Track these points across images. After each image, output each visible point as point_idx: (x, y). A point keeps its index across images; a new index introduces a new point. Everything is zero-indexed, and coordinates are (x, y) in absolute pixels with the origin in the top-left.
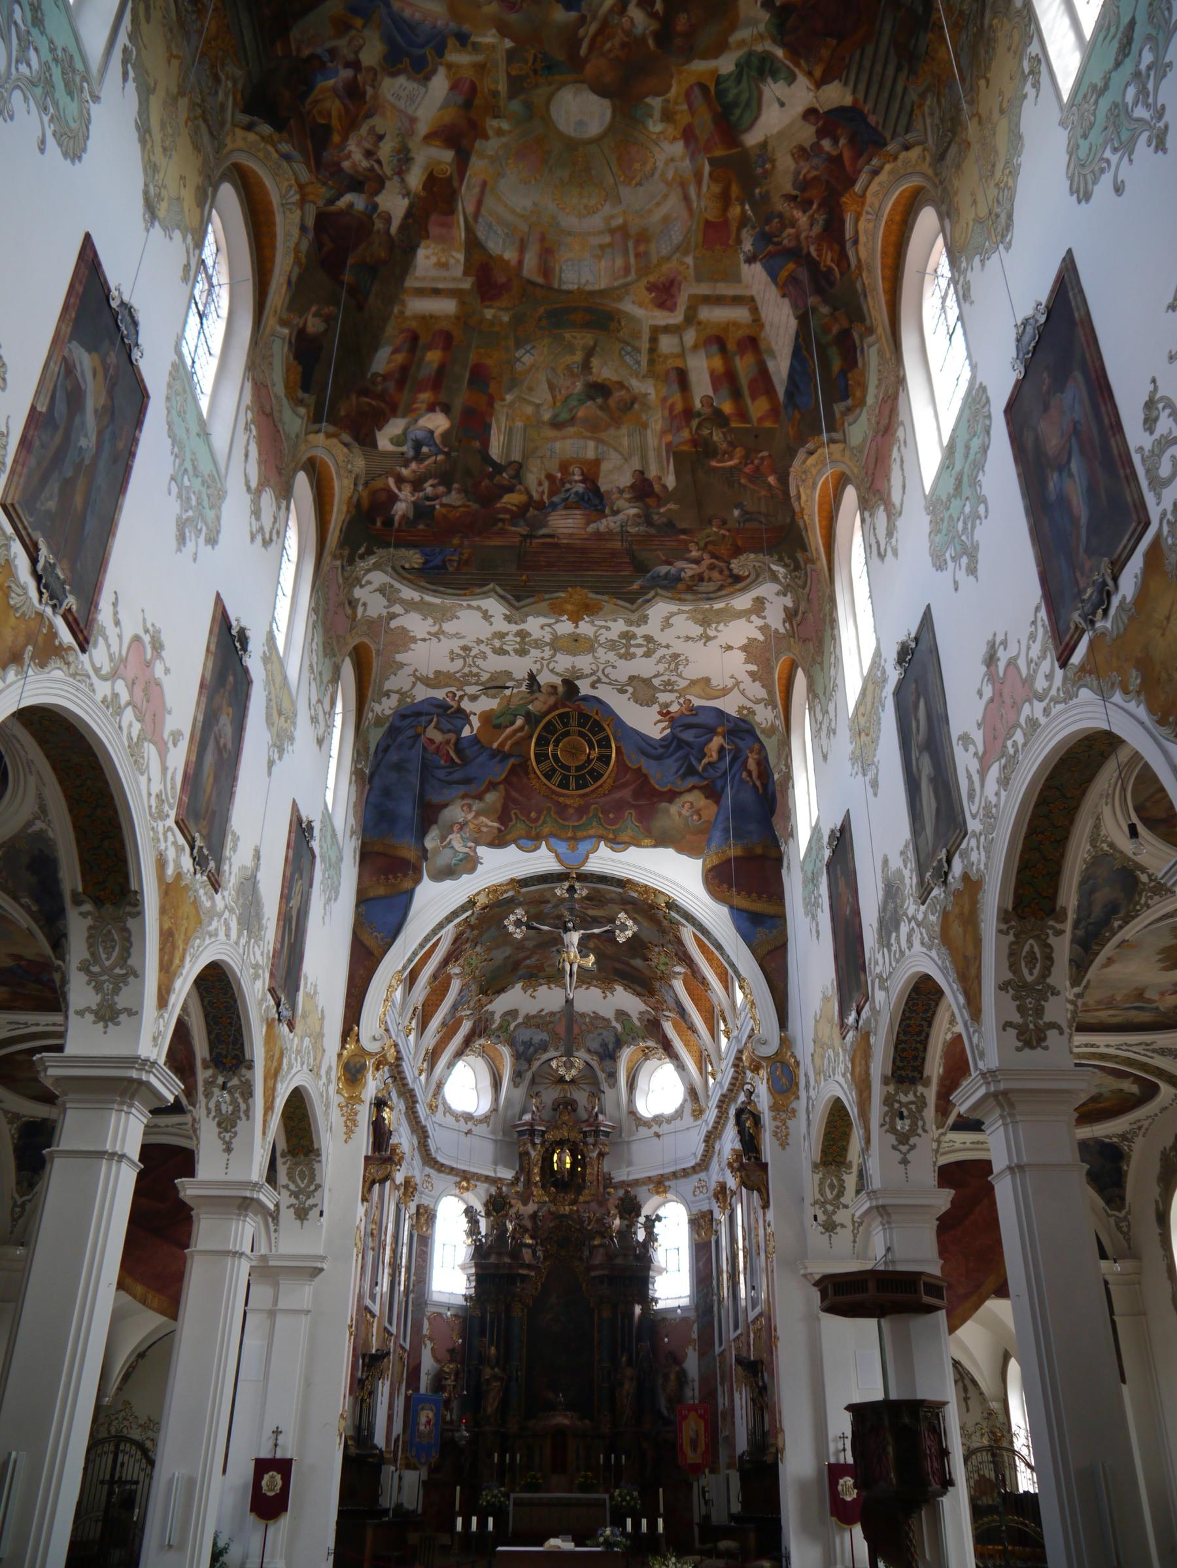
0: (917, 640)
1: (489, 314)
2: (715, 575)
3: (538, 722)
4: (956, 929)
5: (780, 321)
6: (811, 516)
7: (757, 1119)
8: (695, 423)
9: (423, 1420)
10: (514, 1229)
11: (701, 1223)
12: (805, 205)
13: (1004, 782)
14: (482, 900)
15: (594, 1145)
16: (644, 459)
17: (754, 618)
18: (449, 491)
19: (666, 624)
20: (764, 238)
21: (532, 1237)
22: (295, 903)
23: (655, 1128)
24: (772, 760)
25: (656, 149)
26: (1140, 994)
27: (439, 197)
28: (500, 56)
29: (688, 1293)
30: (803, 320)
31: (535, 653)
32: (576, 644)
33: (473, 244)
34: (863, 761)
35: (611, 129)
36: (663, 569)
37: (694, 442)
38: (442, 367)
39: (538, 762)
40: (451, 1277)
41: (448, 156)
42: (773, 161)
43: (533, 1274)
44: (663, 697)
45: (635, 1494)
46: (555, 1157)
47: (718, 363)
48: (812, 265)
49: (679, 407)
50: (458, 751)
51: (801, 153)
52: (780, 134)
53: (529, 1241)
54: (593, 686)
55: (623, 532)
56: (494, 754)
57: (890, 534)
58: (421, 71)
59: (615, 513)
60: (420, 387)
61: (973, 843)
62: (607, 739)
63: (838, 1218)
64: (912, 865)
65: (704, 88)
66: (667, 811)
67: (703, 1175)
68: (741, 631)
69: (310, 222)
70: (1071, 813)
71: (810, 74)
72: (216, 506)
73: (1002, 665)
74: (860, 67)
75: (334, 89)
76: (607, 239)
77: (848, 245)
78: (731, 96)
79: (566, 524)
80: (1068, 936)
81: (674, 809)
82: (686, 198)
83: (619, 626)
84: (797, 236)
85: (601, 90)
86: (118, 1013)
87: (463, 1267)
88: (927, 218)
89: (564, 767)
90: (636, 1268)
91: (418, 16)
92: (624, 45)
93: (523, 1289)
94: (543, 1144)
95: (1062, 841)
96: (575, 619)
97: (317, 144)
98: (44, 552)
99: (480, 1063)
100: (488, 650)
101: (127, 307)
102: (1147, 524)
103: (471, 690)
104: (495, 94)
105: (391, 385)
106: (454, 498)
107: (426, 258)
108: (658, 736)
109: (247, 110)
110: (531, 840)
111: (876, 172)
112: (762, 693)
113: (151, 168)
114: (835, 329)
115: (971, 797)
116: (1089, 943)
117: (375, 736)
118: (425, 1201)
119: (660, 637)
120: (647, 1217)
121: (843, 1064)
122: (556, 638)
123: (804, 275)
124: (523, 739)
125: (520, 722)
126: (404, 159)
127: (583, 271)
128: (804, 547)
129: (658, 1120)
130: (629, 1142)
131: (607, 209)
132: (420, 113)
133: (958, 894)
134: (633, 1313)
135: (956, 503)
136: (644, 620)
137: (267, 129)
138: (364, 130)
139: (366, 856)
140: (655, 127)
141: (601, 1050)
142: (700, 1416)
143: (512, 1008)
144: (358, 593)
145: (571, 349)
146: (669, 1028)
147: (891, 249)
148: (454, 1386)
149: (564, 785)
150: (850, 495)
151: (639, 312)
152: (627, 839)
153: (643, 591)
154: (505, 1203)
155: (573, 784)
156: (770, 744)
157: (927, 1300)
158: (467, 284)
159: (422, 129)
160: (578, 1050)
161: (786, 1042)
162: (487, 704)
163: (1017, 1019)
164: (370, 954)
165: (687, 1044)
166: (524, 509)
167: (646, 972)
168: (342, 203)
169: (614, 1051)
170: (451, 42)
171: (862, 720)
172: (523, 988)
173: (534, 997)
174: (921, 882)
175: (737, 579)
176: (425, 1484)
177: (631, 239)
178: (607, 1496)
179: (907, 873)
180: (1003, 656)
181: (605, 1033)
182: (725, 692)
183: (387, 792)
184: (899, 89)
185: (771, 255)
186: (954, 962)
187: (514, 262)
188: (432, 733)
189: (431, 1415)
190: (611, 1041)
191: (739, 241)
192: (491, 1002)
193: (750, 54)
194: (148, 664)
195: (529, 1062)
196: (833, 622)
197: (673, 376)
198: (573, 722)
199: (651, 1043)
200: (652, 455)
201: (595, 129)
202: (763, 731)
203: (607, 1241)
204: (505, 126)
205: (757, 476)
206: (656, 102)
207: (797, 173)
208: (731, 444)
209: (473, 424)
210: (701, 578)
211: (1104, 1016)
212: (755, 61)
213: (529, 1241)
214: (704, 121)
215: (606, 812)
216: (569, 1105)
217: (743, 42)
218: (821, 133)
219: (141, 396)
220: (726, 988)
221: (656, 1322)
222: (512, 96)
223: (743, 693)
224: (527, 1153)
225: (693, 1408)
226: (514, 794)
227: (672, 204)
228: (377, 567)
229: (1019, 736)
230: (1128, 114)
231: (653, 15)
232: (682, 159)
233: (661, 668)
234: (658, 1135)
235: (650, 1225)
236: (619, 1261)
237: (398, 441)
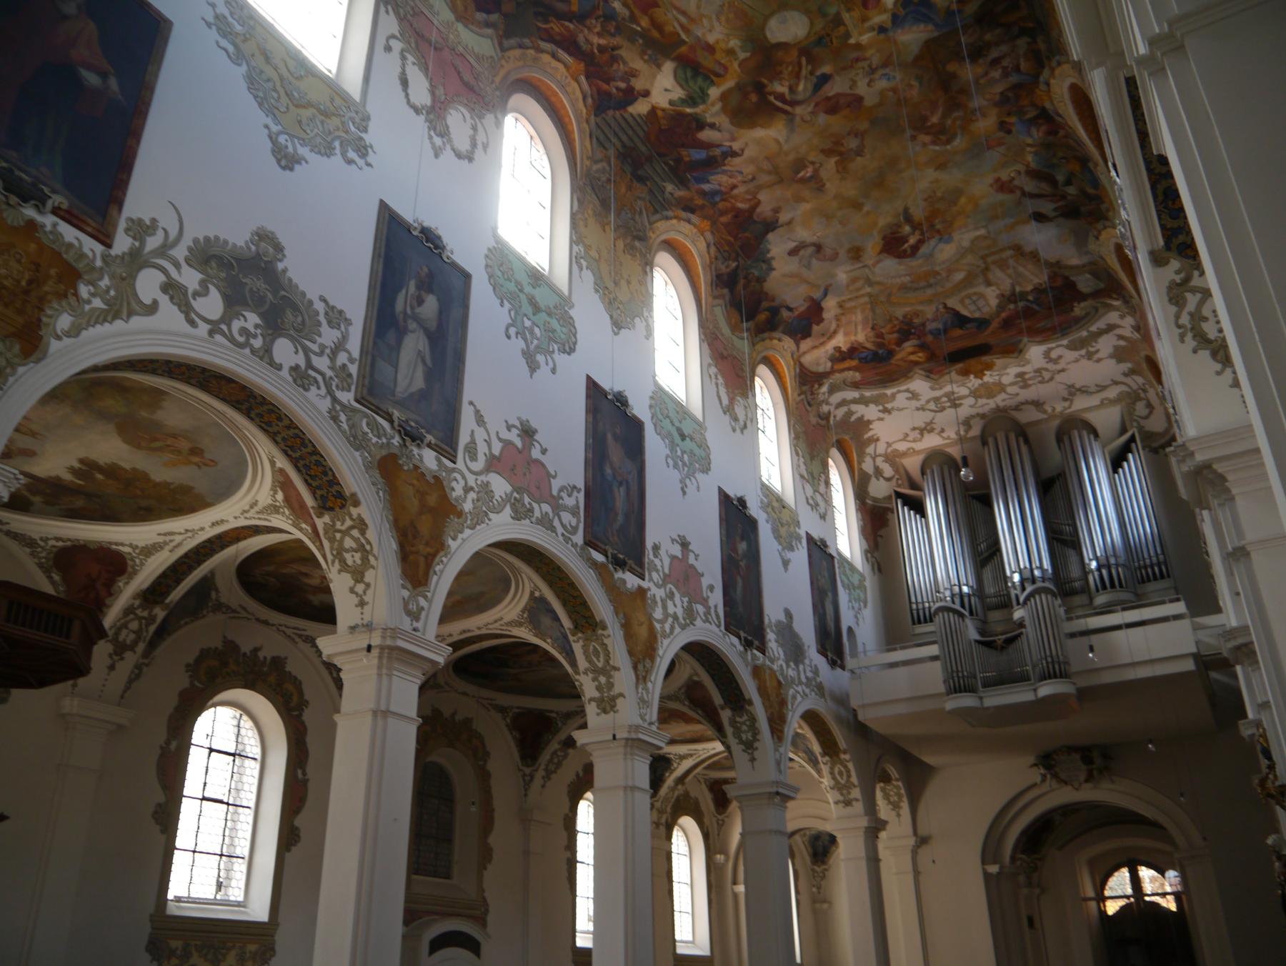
12: (602, 49)
28: (854, 33)
35: (762, 28)
42: (645, 61)
48: (561, 16)
51: (633, 74)
52: (654, 77)
65: (718, 75)
71: (663, 110)
77: (554, 47)
78: (700, 80)
82: (684, 13)
84: (589, 29)
91: (915, 28)
92: (781, 72)
104: (849, 10)
111: (584, 98)
140: (734, 43)
170: (889, 24)
191: (625, 5)
193: (704, 102)
201: (773, 23)
207: (625, 63)
214: (706, 61)
217: (713, 104)
222: (838, 14)
231: (770, 94)
232: (704, 34)
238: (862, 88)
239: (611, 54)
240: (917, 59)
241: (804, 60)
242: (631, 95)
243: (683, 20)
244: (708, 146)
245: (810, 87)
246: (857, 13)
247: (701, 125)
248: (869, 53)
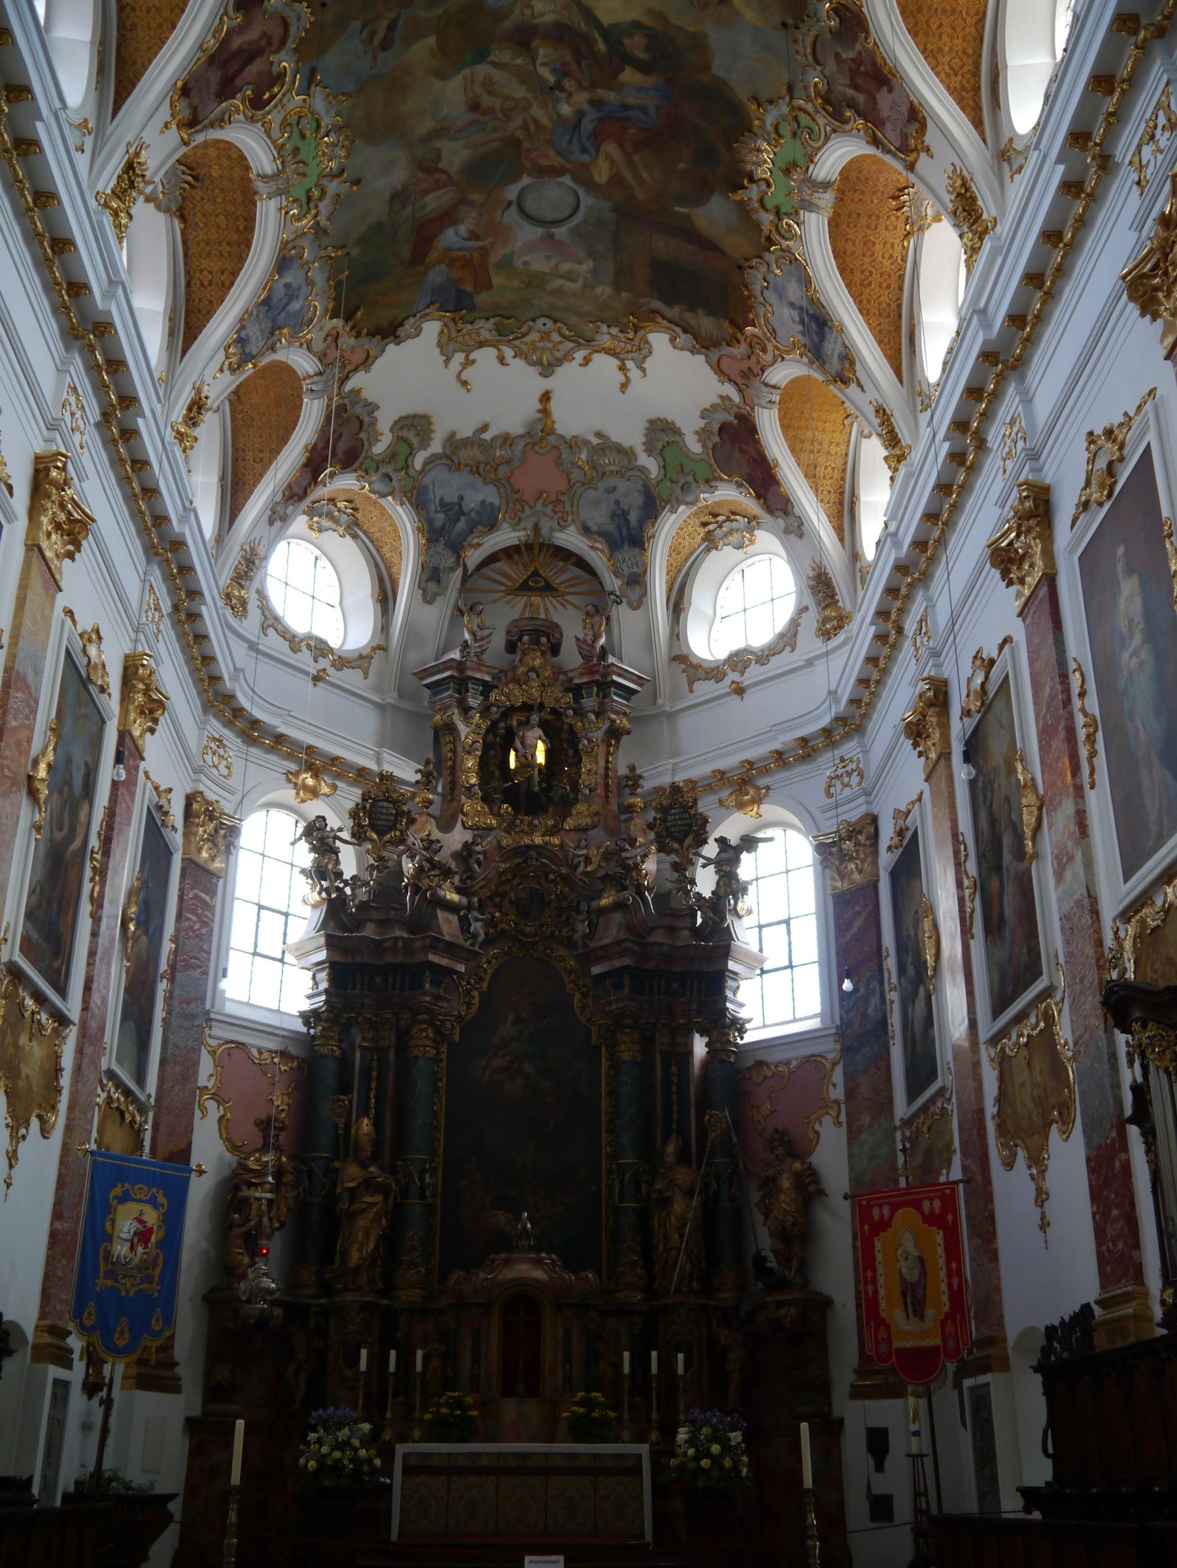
9: (125, 1227)
10: (420, 870)
11: (846, 849)
15: (597, 715)
21: (459, 891)
23: (736, 676)
29: (817, 1009)
40: (269, 962)
43: (461, 968)
45: (736, 1437)
53: (454, 897)
67: (850, 748)
87: (301, 952)
90: (693, 960)
93: (439, 998)
94: (485, 711)
99: (348, 550)
120: (722, 842)
129: (739, 660)
130: (672, 716)
134: (690, 1053)
141: (611, 527)
142: (931, 1219)
143: (421, 411)
148: (270, 1201)
154: (400, 814)
160: (562, 528)
165: (811, 475)
167: (735, 245)
169: (642, 524)
172: (440, 345)
173: (464, 383)
176: (190, 1423)
178: (644, 1449)
181: (622, 485)
189: (152, 1217)
190: (634, 502)
192: (367, 362)
195: (457, 549)
203: (629, 896)
213: (454, 897)
216: (547, 638)
220: (978, 123)
221: (742, 1073)
224: (451, 728)
234: (739, 691)
235: (729, 855)
236: (658, 937)
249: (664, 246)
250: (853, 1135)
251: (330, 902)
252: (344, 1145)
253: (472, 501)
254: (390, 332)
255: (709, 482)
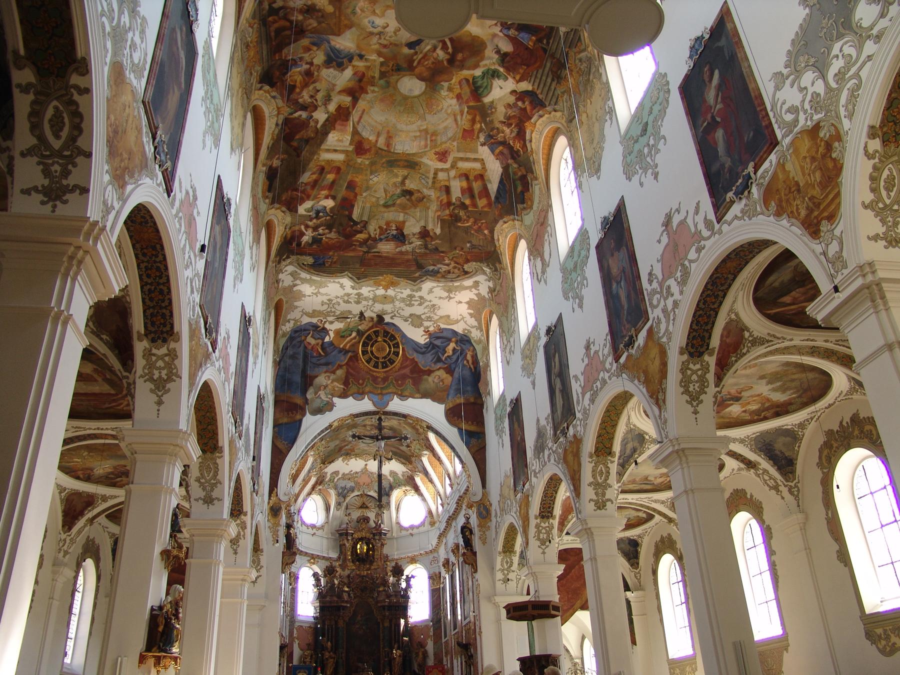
0: (555, 327)
1: (359, 160)
2: (456, 271)
3: (363, 334)
4: (570, 458)
5: (494, 169)
6: (504, 249)
7: (471, 532)
8: (452, 208)
11: (435, 578)
12: (509, 125)
13: (592, 401)
14: (336, 424)
16: (426, 221)
17: (473, 289)
18: (331, 232)
19: (431, 291)
20: (490, 137)
22: (258, 435)
24: (479, 356)
25: (444, 102)
26: (646, 478)
27: (342, 114)
28: (378, 64)
30: (506, 169)
31: (364, 303)
32: (385, 299)
33: (355, 132)
34: (528, 370)
36: (431, 268)
37: (451, 216)
38: (333, 182)
39: (363, 354)
40: (307, 607)
41: (348, 99)
42: (496, 108)
44: (426, 324)
46: (359, 546)
47: (465, 184)
48: (511, 148)
49: (445, 201)
50: (323, 348)
51: (509, 106)
52: (500, 99)
54: (392, 318)
55: (413, 252)
56: (341, 351)
57: (543, 272)
58: (341, 67)
59: (410, 243)
60: (323, 189)
61: (578, 423)
62: (398, 343)
63: (509, 577)
64: (551, 425)
65: (467, 80)
66: (427, 380)
67: (436, 555)
68: (467, 295)
69: (280, 122)
70: (619, 415)
72: (242, 264)
73: (592, 352)
74: (536, 77)
75: (300, 73)
76: (418, 134)
77: (527, 142)
78: (479, 83)
79: (386, 248)
80: (616, 463)
81: (430, 379)
82: (456, 120)
83: (408, 292)
84: (504, 137)
85: (421, 78)
86: (213, 500)
88: (562, 141)
89: (376, 357)
91: (342, 48)
92: (433, 63)
95: (614, 426)
96: (386, 288)
97: (289, 93)
98: (210, 320)
100: (341, 301)
101: (229, 200)
102: (648, 320)
103: (330, 319)
104: (373, 77)
105: (308, 188)
106: (333, 235)
107: (333, 138)
108: (423, 343)
109: (260, 83)
110: (359, 395)
111: (541, 116)
112: (475, 323)
113: (232, 128)
114: (520, 174)
115: (578, 403)
116: (623, 465)
117: (282, 341)
118: (293, 570)
119: (427, 297)
121: (515, 508)
122: (375, 296)
123: (506, 151)
124: (355, 343)
125: (354, 334)
126: (328, 99)
127: (405, 145)
128: (500, 263)
129: (412, 527)
131: (419, 123)
132: (338, 83)
133: (571, 442)
135: (574, 274)
136: (420, 289)
137: (267, 88)
138: (311, 88)
139: (277, 402)
140: (444, 93)
144: (281, 276)
145: (396, 176)
146: (418, 480)
147: (546, 147)
149: (376, 366)
150: (523, 244)
151: (429, 163)
152: (407, 394)
153: (420, 277)
155: (380, 366)
156: (479, 348)
157: (553, 612)
158: (351, 148)
159: (338, 88)
161: (485, 495)
162: (338, 325)
163: (595, 498)
164: (281, 452)
166: (365, 241)
167: (409, 453)
168: (297, 115)
170: (355, 58)
171: (528, 352)
174: (555, 434)
175: (466, 273)
177: (430, 135)
179: (548, 428)
180: (593, 349)
182: (457, 322)
183: (287, 370)
184: (553, 87)
185: (492, 143)
186: (569, 471)
187: (374, 141)
188: (310, 339)
191: (478, 137)
194: (226, 348)
195: (345, 497)
196: (514, 301)
197: (444, 188)
198: (381, 335)
199: (408, 488)
200: (430, 220)
201: (417, 92)
202: (475, 341)
204: (376, 89)
205: (480, 230)
206: (446, 84)
208: (468, 217)
209: (346, 205)
210: (449, 272)
211: (631, 487)
212: (491, 72)
214: (466, 91)
215: (397, 380)
216: (367, 519)
218: (517, 99)
219: (230, 232)
222: (380, 78)
223: (465, 322)
224: (344, 545)
225: (433, 667)
226: (351, 371)
227: (450, 121)
228: (290, 264)
229: (598, 384)
230: (645, 159)
231: (448, 53)
233: (426, 311)
235: (408, 580)
237: (308, 210)
238: (393, 24)
239: (507, 122)
240: (350, 27)
241: (415, 64)
242: (521, 96)
243: (459, 118)
244: (513, 40)
245: (423, 45)
246: (370, 73)
247: (504, 58)
248: (377, 46)
249: (393, 449)
250: (434, 644)
251: (320, 593)
252: (323, 648)
253: (348, 486)
254: (333, 461)
255: (405, 485)
